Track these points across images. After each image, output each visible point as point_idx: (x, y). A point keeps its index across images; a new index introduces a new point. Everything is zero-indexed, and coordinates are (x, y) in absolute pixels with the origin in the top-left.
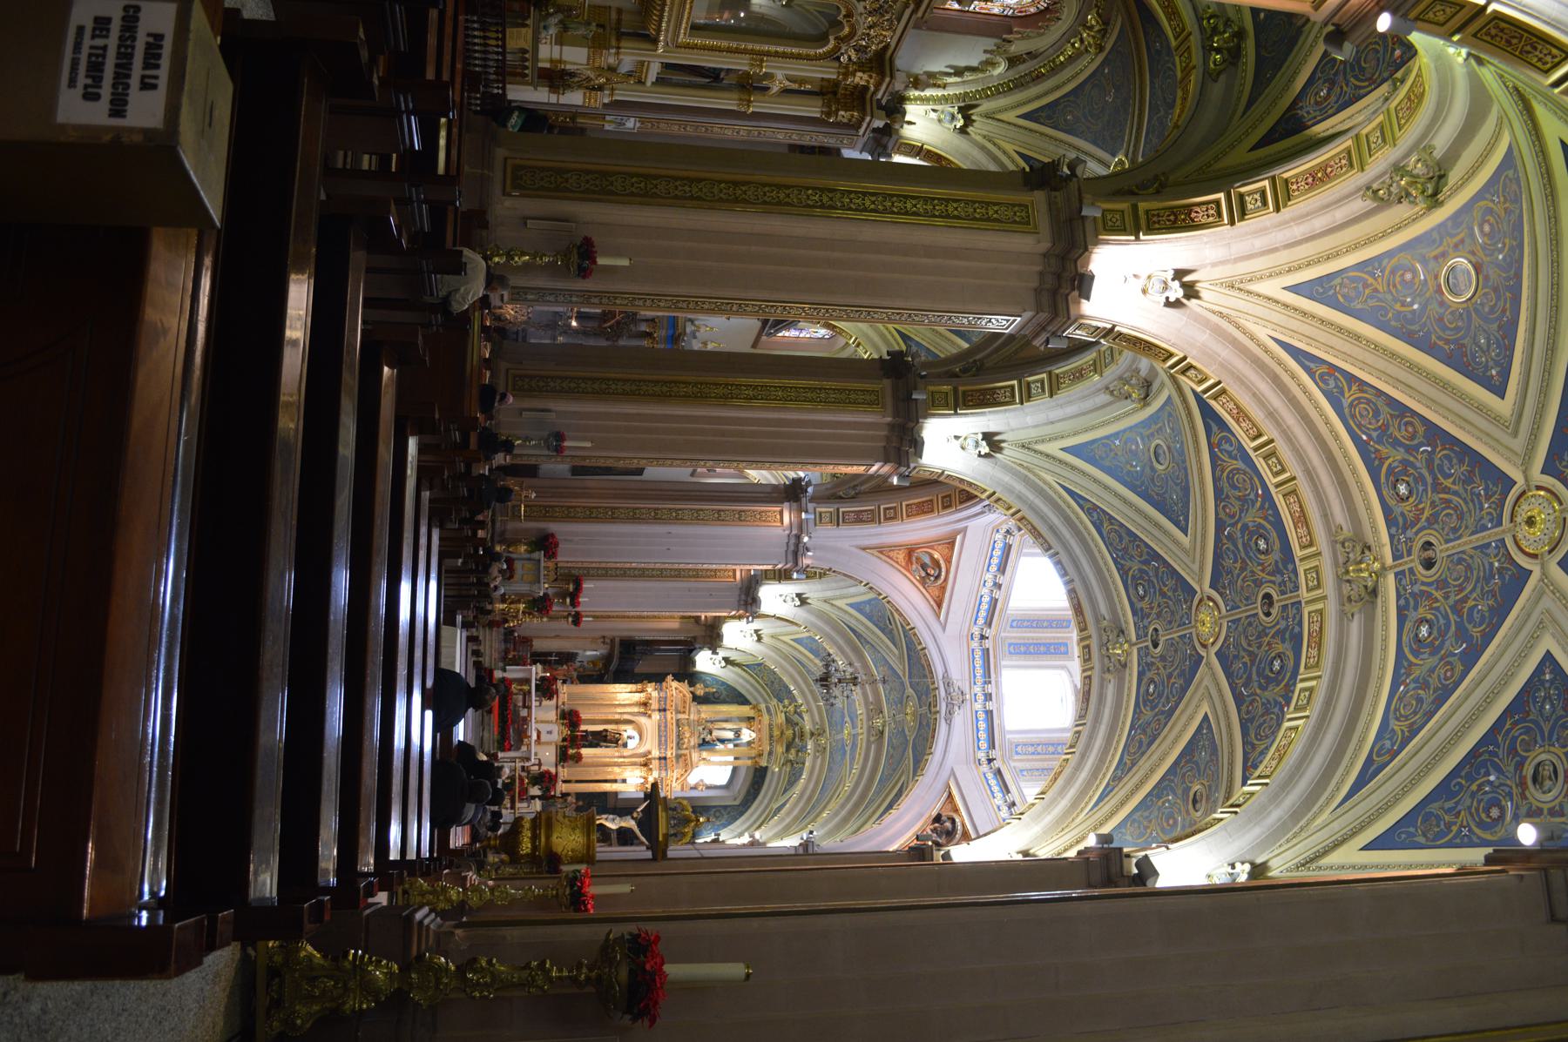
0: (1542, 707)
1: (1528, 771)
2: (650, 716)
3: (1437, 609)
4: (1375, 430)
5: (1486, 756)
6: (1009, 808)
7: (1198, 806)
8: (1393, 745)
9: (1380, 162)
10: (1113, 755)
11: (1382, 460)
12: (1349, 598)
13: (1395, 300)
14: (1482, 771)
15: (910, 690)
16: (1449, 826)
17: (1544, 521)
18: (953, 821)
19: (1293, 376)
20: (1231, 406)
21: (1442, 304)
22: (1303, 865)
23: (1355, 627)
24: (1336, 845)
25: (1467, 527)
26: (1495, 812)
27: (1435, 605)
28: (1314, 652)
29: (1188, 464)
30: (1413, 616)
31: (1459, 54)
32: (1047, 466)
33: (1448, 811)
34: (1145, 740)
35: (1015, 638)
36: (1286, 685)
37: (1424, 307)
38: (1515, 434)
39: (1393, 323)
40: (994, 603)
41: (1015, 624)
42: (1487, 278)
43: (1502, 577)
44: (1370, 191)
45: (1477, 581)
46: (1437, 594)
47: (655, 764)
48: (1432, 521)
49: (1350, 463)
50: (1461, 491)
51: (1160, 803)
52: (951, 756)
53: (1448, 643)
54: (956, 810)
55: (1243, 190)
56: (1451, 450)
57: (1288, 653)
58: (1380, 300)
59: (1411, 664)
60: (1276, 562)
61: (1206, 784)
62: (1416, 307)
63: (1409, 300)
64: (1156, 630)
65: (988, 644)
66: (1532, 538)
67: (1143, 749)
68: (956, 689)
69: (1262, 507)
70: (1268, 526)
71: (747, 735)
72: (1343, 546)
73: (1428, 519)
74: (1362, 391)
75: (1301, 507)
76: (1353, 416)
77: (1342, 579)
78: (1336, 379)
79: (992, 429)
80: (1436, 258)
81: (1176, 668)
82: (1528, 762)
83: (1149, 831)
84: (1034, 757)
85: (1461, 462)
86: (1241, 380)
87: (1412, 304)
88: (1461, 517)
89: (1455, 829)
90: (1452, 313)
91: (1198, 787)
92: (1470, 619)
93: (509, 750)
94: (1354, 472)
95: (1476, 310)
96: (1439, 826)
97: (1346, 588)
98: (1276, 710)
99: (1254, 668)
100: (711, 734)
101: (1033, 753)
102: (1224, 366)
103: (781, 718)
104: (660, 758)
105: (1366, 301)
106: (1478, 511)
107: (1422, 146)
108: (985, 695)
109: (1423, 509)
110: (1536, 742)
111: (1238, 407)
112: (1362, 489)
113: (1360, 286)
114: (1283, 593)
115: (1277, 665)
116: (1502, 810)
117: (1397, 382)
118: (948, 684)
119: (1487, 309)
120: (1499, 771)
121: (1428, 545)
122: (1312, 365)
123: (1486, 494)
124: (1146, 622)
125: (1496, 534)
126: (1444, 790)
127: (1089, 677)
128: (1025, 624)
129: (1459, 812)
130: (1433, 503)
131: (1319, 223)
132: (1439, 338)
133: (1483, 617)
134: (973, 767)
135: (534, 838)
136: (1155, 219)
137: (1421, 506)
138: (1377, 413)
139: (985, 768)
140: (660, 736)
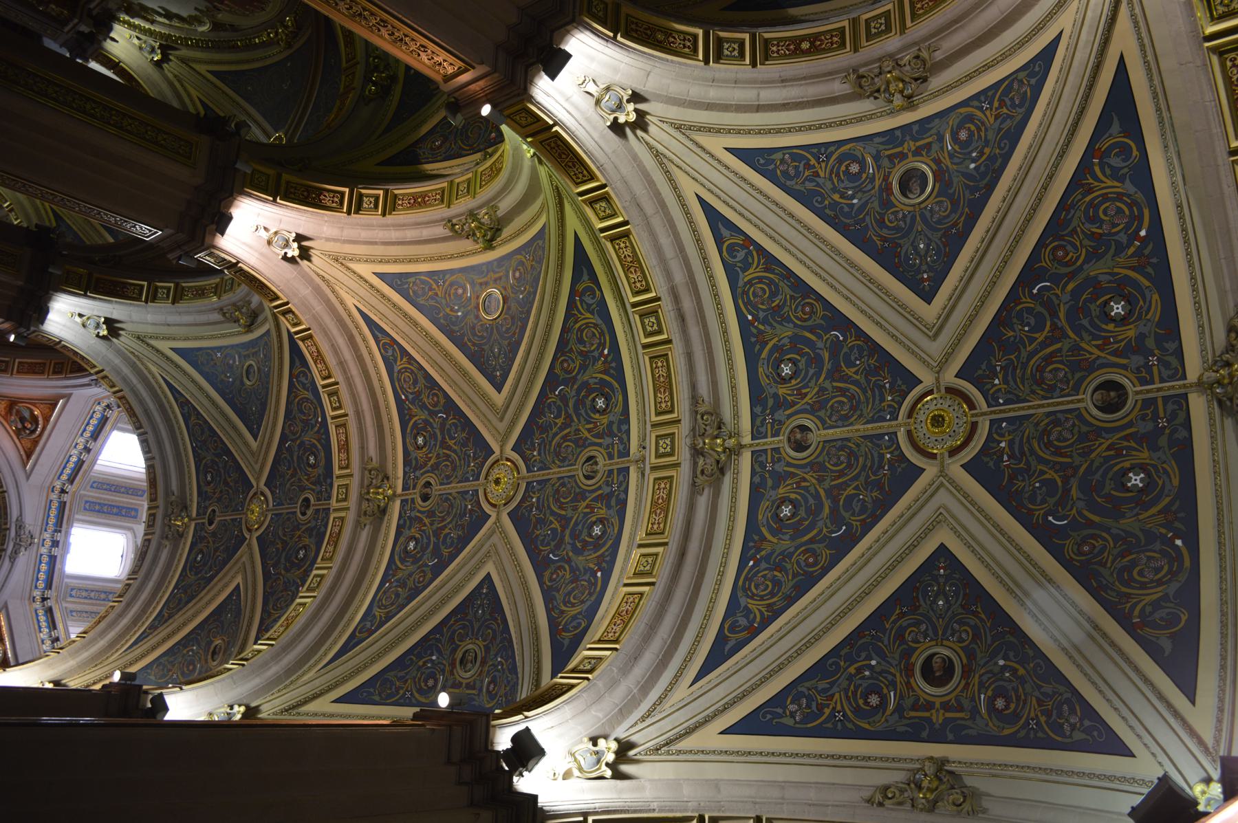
0: (477, 611)
1: (459, 655)
3: (424, 531)
6: (53, 642)
7: (216, 656)
8: (372, 626)
9: (463, 205)
11: (411, 417)
12: (365, 512)
13: (448, 306)
14: (429, 652)
16: (398, 689)
17: (506, 483)
19: (364, 340)
20: (314, 349)
21: (477, 317)
22: (286, 711)
23: (364, 535)
24: (315, 697)
28: (331, 548)
30: (407, 533)
31: (529, 151)
32: (155, 359)
33: (399, 679)
35: (93, 497)
36: (305, 571)
37: (465, 316)
38: (501, 419)
39: (442, 321)
40: (80, 464)
41: (95, 485)
42: (509, 308)
43: (471, 517)
44: (450, 223)
46: (427, 521)
48: (435, 467)
49: (389, 413)
50: (459, 451)
51: (185, 652)
53: (425, 557)
55: (363, 191)
56: (459, 420)
58: (437, 302)
59: (398, 568)
60: (319, 475)
62: (460, 314)
64: (214, 511)
65: (66, 498)
66: (496, 492)
69: (318, 432)
70: (319, 447)
73: (432, 465)
74: (410, 364)
75: (346, 438)
77: (362, 498)
78: (394, 349)
79: (115, 316)
80: (481, 284)
84: (86, 601)
85: (463, 430)
87: (458, 311)
88: (454, 469)
89: (401, 692)
92: (444, 542)
94: (390, 420)
97: (365, 505)
98: (293, 589)
99: (284, 555)
101: (86, 598)
102: (315, 318)
107: (491, 204)
110: (468, 635)
111: (318, 352)
112: (393, 435)
114: (319, 500)
115: (302, 553)
116: (436, 681)
117: (434, 363)
118: (20, 526)
120: (440, 653)
121: (428, 484)
122: (380, 335)
124: (207, 503)
125: (474, 485)
126: (399, 663)
127: (149, 540)
129: (407, 681)
130: (438, 454)
131: (411, 234)
132: (469, 340)
134: (27, 602)
136: (292, 190)
138: (415, 382)
139: (38, 605)
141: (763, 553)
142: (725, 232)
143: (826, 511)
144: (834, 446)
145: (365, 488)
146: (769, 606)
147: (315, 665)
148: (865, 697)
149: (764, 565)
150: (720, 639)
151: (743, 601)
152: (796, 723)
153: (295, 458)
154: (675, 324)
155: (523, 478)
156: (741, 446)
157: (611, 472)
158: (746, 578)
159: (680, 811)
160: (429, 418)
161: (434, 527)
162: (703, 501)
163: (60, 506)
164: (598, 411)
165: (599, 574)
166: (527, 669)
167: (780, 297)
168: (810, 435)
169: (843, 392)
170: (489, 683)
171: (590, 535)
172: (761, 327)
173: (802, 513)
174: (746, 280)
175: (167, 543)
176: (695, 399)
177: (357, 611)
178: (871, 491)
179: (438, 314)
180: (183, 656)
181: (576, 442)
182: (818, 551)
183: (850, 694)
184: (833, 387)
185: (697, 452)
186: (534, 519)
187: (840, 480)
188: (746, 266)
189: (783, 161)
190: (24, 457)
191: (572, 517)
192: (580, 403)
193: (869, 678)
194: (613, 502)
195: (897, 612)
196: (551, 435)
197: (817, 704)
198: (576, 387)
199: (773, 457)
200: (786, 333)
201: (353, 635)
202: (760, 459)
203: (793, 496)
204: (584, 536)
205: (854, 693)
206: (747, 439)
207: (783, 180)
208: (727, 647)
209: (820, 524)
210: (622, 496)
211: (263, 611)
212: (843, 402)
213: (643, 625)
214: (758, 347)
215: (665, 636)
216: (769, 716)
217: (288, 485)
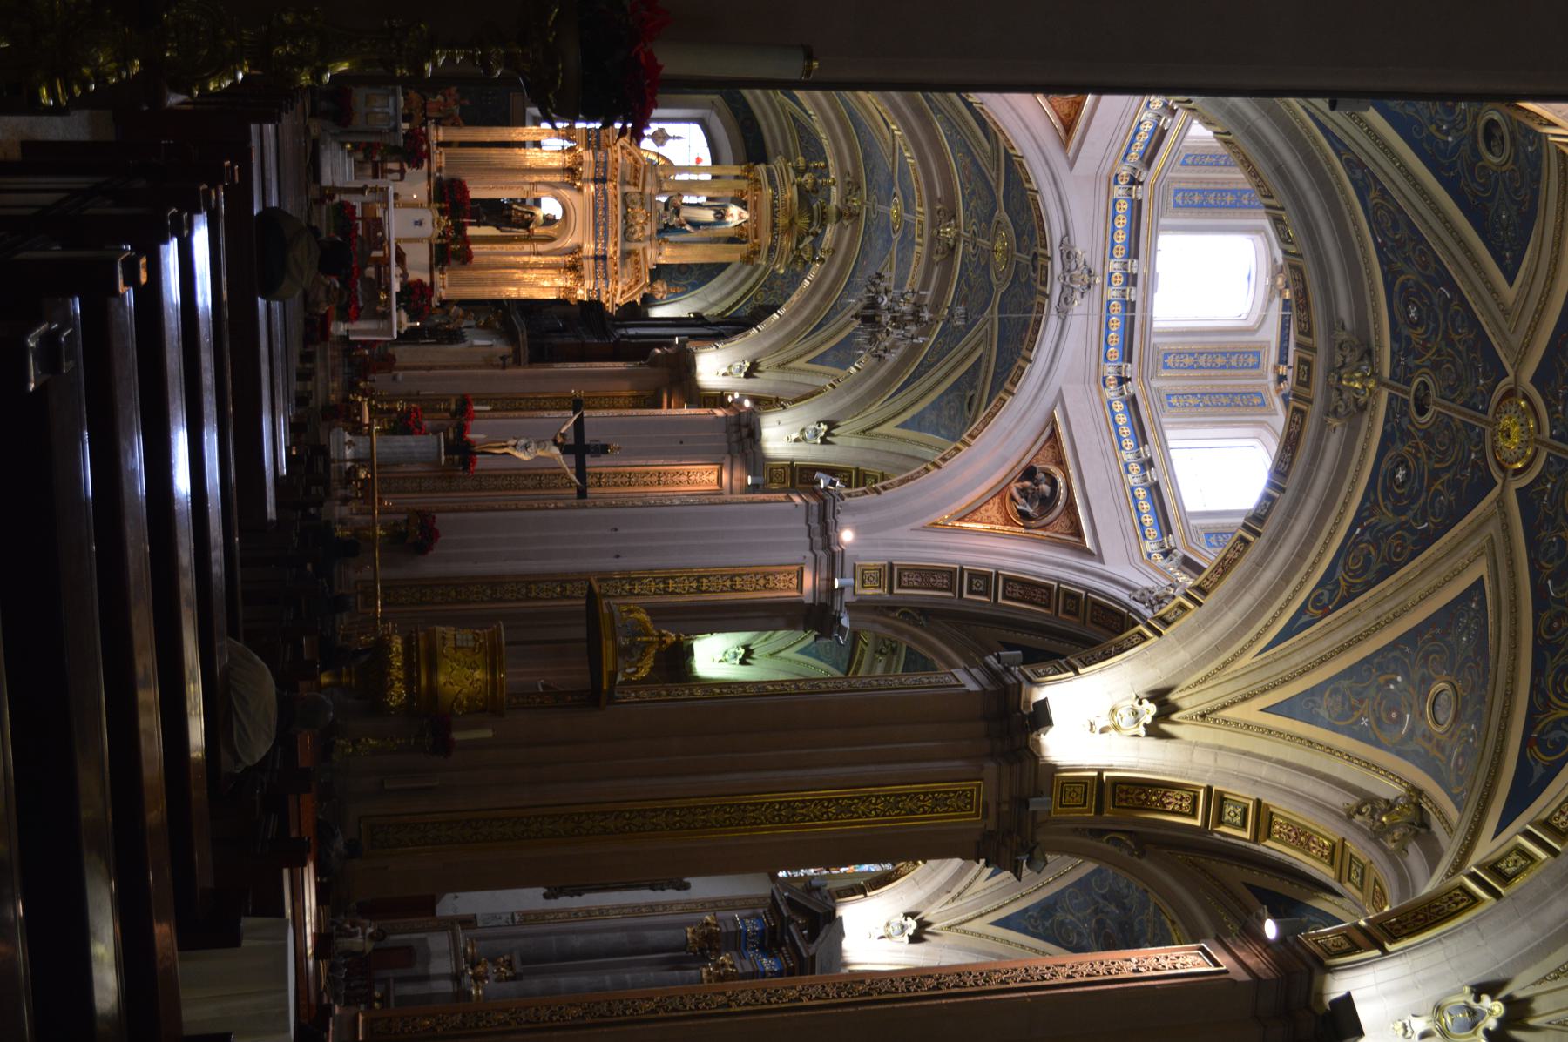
2: (580, 190)
10: (1320, 555)
15: (1004, 214)
18: (1053, 483)
29: (1543, 186)
34: (1375, 567)
35: (1187, 180)
41: (1189, 161)
47: (588, 265)
51: (1382, 680)
52: (1057, 380)
54: (1060, 462)
61: (1460, 692)
64: (1424, 383)
65: (1139, 192)
67: (1370, 575)
71: (735, 215)
81: (1447, 470)
83: (1357, 714)
91: (1442, 685)
93: (357, 318)
100: (677, 213)
101: (1191, 367)
103: (792, 193)
104: (596, 258)
108: (1127, 276)
118: (1068, 255)
134: (1094, 387)
135: (410, 681)
139: (1111, 392)
140: (596, 225)
163: (1131, 208)
180: (1379, 689)
190: (1062, 133)
211: (1534, 687)
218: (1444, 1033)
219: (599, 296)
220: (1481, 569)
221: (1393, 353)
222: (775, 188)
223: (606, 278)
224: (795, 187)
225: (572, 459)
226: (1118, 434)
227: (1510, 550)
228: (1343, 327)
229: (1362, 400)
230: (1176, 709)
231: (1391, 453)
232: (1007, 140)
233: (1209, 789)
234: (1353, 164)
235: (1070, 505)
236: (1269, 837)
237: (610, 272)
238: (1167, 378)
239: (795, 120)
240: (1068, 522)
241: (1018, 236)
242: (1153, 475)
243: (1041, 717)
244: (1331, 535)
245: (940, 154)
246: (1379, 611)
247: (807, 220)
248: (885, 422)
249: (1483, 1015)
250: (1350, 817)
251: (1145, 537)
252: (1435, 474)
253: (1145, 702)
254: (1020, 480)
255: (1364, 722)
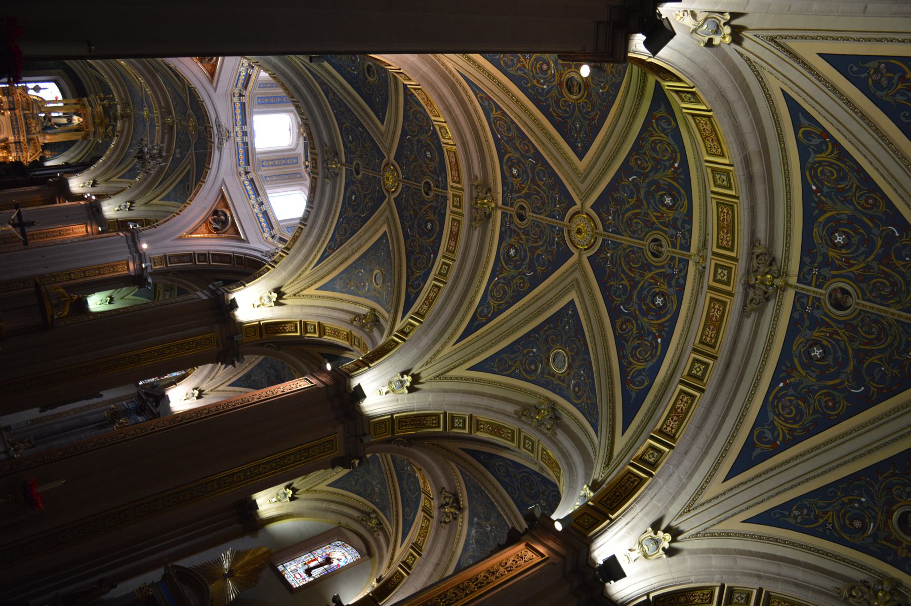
0: (564, 326)
2: (3, 114)
3: (521, 244)
4: (506, 136)
5: (533, 339)
11: (506, 152)
13: (534, 77)
15: (191, 111)
16: (510, 367)
18: (226, 215)
23: (476, 234)
25: (545, 211)
26: (533, 367)
27: (520, 241)
33: (511, 359)
34: (349, 231)
35: (261, 94)
36: (434, 241)
37: (549, 90)
38: (583, 182)
39: (530, 90)
41: (261, 86)
45: (545, 242)
46: (523, 237)
47: (13, 146)
48: (527, 196)
50: (546, 191)
51: (356, 272)
52: (221, 175)
53: (524, 267)
54: (227, 207)
57: (436, 222)
58: (525, 73)
59: (503, 267)
60: (435, 168)
62: (545, 87)
63: (542, 81)
65: (243, 99)
68: (224, 129)
70: (434, 148)
71: (76, 120)
72: (477, 189)
73: (525, 194)
75: (456, 160)
76: (495, 124)
78: (489, 103)
82: (552, 350)
83: (349, 286)
84: (274, 168)
85: (550, 178)
86: (432, 86)
87: (543, 84)
89: (513, 369)
90: (564, 101)
91: (377, 271)
92: (538, 261)
95: (578, 107)
96: (505, 365)
99: (416, 221)
100: (50, 120)
101: (272, 165)
102: (424, 77)
103: (100, 109)
104: (15, 143)
105: (517, 70)
106: (553, 207)
109: (523, 188)
113: (515, 59)
118: (219, 126)
119: (585, 111)
120: (539, 349)
121: (522, 208)
122: (477, 90)
123: (559, 201)
128: (268, 85)
129: (516, 362)
132: (554, 111)
133: (544, 263)
134: (236, 176)
137: (523, 186)
139: (243, 178)
140: (13, 129)
141: (792, 380)
142: (803, 121)
143: (850, 368)
144: (869, 317)
145: (474, 199)
146: (790, 430)
147: (449, 339)
148: (852, 520)
149: (791, 391)
150: (749, 445)
151: (771, 416)
152: (797, 522)
153: (415, 149)
154: (743, 186)
155: (601, 235)
156: (787, 285)
157: (673, 258)
158: (775, 397)
159: (709, 582)
160: (521, 158)
161: (530, 244)
162: (748, 323)
163: (241, 105)
164: (665, 205)
165: (659, 340)
166: (604, 411)
167: (846, 183)
168: (850, 300)
169: (888, 276)
170: (575, 386)
171: (653, 303)
172: (822, 198)
173: (830, 360)
174: (816, 159)
175: (328, 181)
176: (753, 242)
177: (476, 293)
178: (892, 368)
179: (527, 84)
181: (646, 222)
182: (838, 399)
183: (840, 515)
184: (879, 269)
185: (748, 286)
186: (608, 272)
187: (868, 347)
188: (819, 150)
189: (877, 70)
190: (210, 78)
191: (639, 282)
192: (649, 194)
193: (857, 508)
194: (673, 283)
195: (891, 471)
196: (624, 209)
197: (815, 515)
198: (647, 181)
199: (813, 303)
200: (846, 211)
201: (474, 318)
202: (802, 300)
203: (825, 343)
204: (648, 301)
205: (844, 515)
206: (793, 280)
207: (873, 89)
208: (755, 453)
209: (843, 376)
210: (681, 281)
211: (408, 267)
212: (886, 285)
213: (694, 427)
214: (816, 212)
215: (709, 433)
216: (778, 515)
217: (412, 166)
218: (393, 391)
219: (20, 159)
220: (385, 228)
221: (345, 153)
222: (92, 107)
223: (22, 151)
224: (101, 107)
225: (19, 229)
226: (248, 194)
227: (394, 219)
228: (326, 145)
229: (336, 171)
230: (284, 294)
231: (349, 190)
232: (188, 81)
233: (301, 322)
234: (322, 84)
235: (233, 223)
236: (325, 335)
237: (23, 149)
238: (265, 170)
239: (97, 77)
240: (233, 230)
241: (198, 120)
242: (264, 208)
243: (234, 305)
244: (332, 222)
245: (161, 88)
246: (352, 248)
247: (108, 120)
248: (154, 199)
249: (405, 382)
250: (352, 323)
251: (264, 232)
252: (365, 196)
253: (272, 293)
254: (213, 215)
255: (352, 288)
